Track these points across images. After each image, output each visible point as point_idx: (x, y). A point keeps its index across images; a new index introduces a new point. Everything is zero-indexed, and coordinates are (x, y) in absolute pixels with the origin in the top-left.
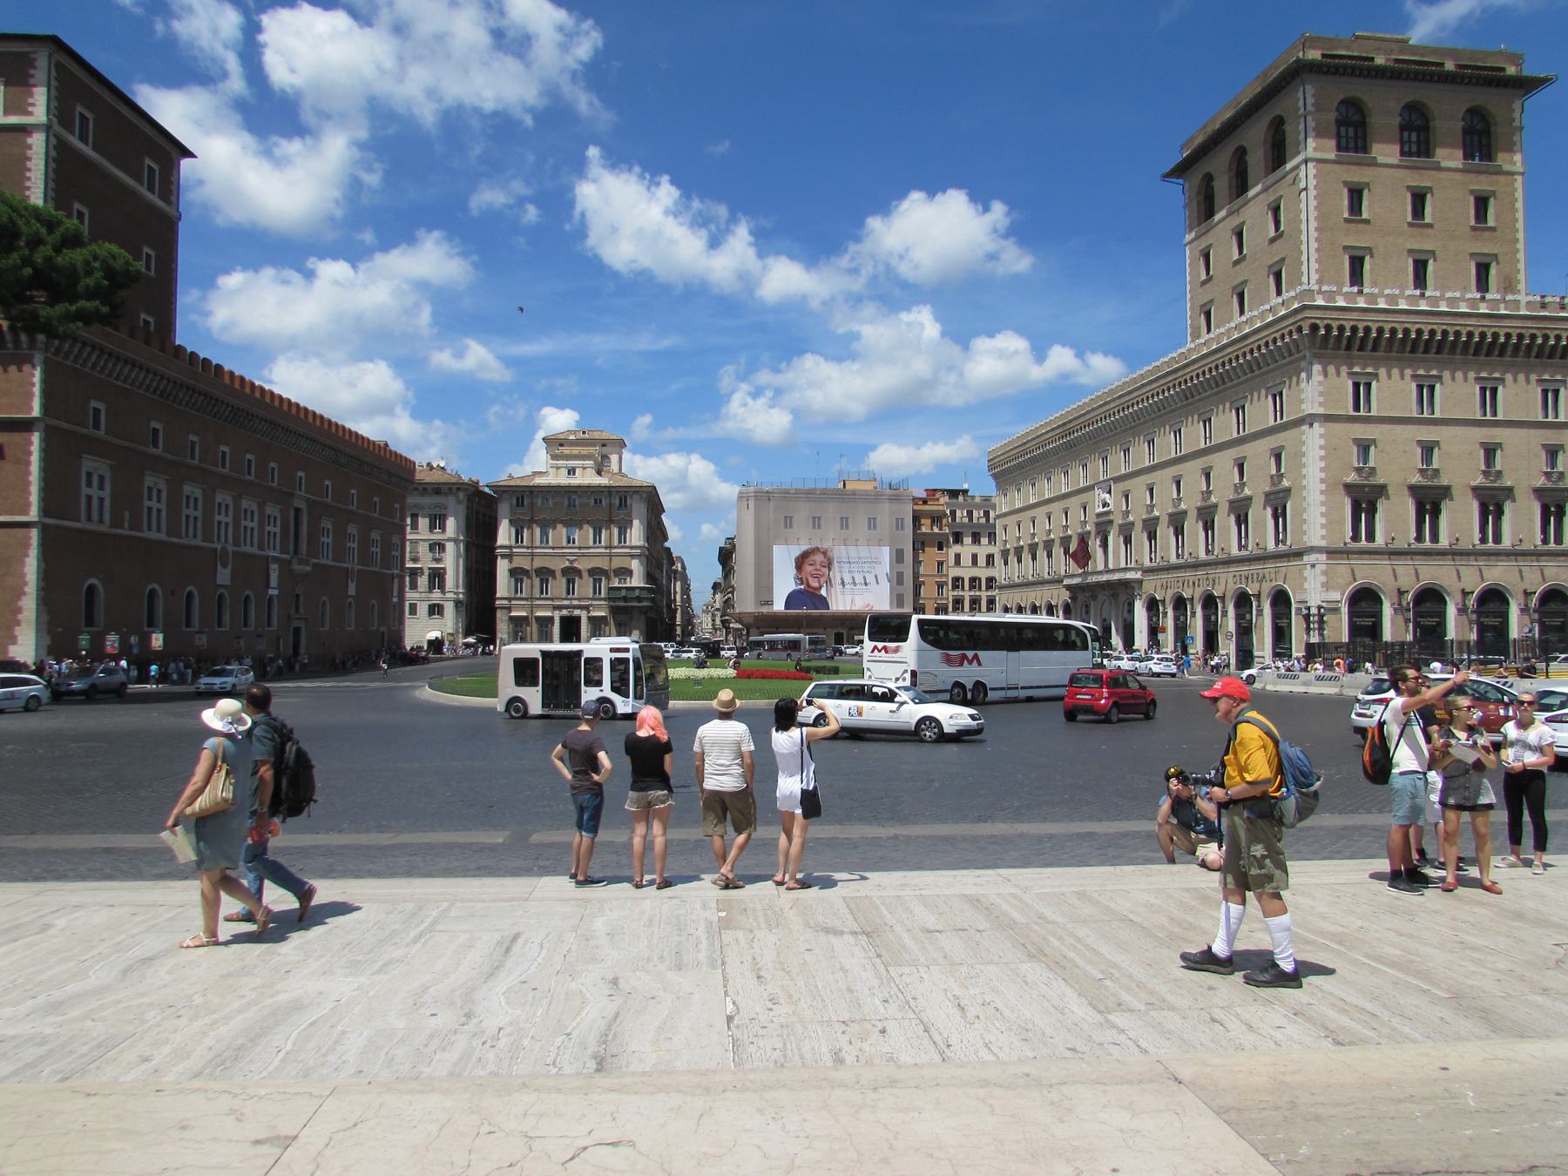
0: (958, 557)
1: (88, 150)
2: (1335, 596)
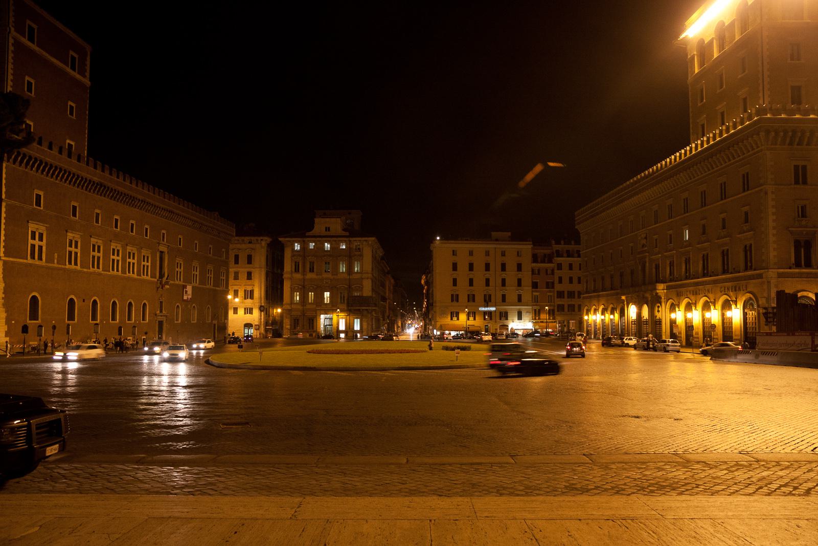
1: (34, 47)
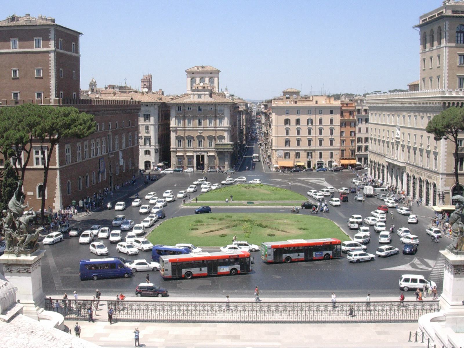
0: (360, 129)
1: (61, 51)
2: (448, 188)
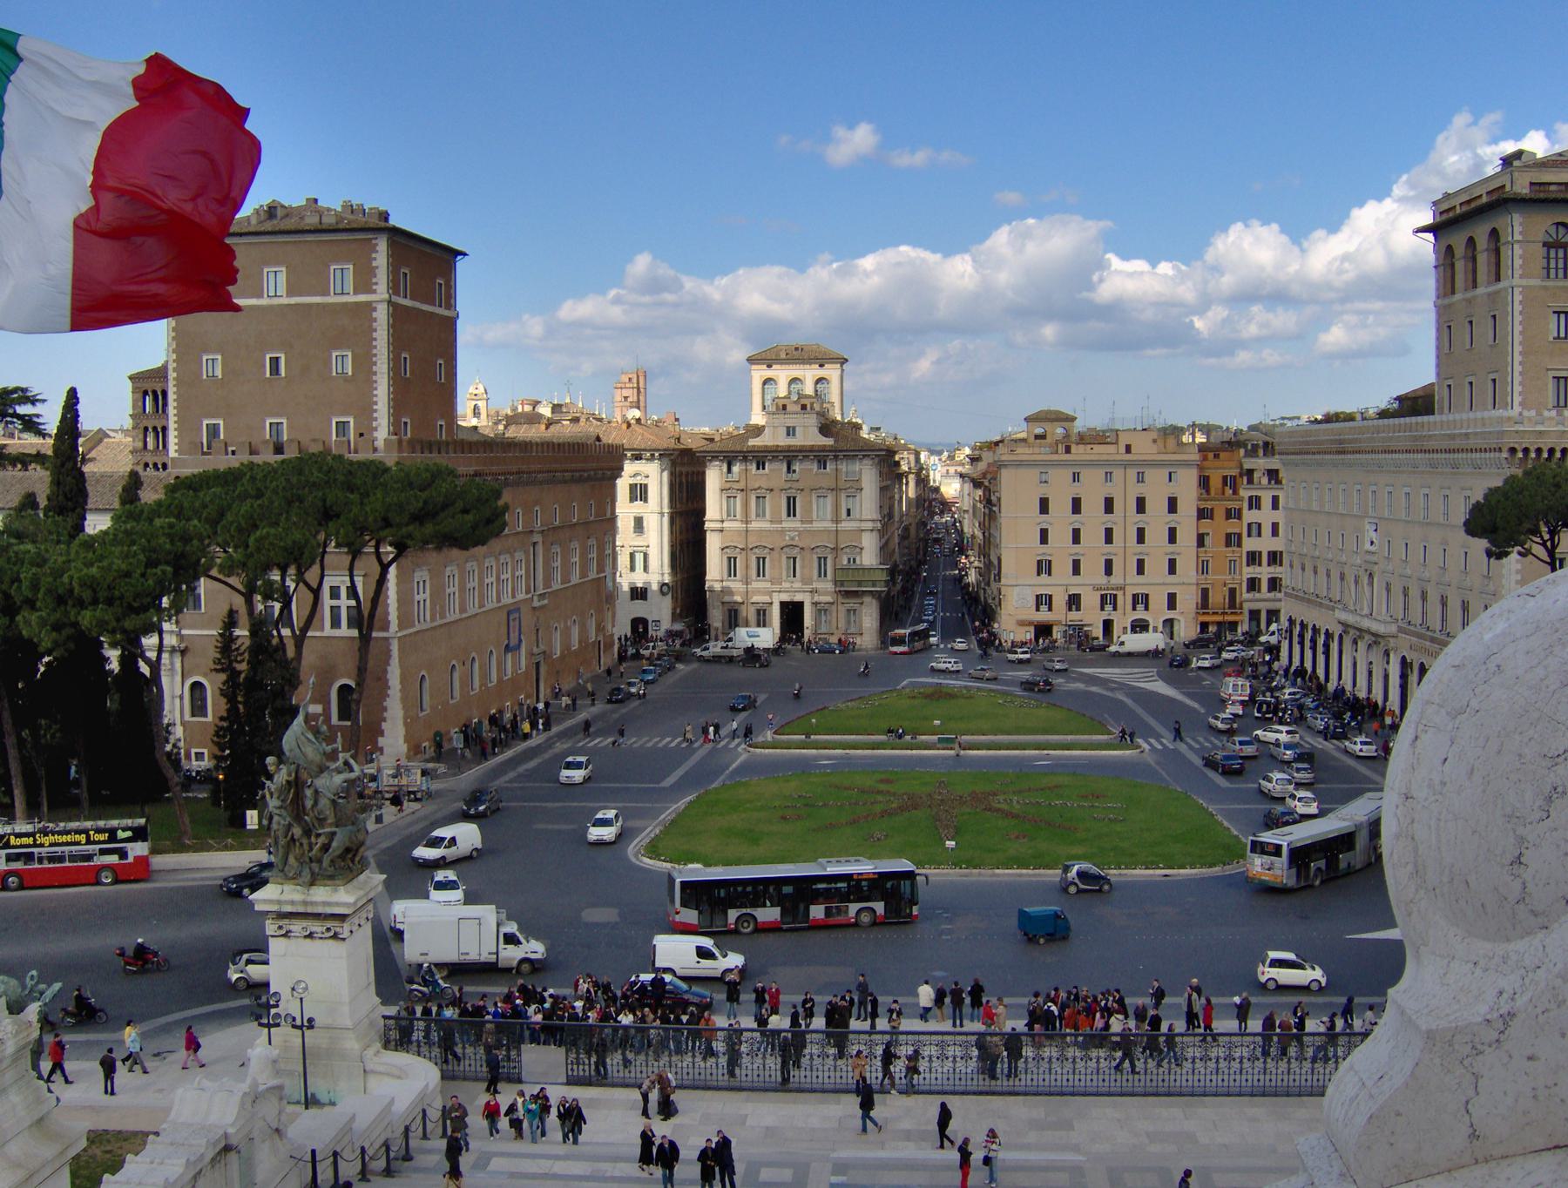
1: (407, 302)
